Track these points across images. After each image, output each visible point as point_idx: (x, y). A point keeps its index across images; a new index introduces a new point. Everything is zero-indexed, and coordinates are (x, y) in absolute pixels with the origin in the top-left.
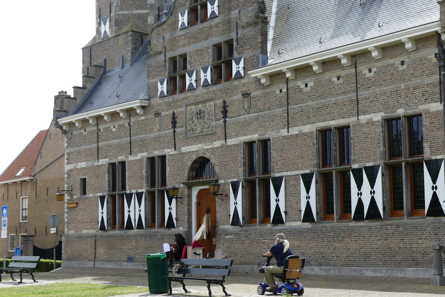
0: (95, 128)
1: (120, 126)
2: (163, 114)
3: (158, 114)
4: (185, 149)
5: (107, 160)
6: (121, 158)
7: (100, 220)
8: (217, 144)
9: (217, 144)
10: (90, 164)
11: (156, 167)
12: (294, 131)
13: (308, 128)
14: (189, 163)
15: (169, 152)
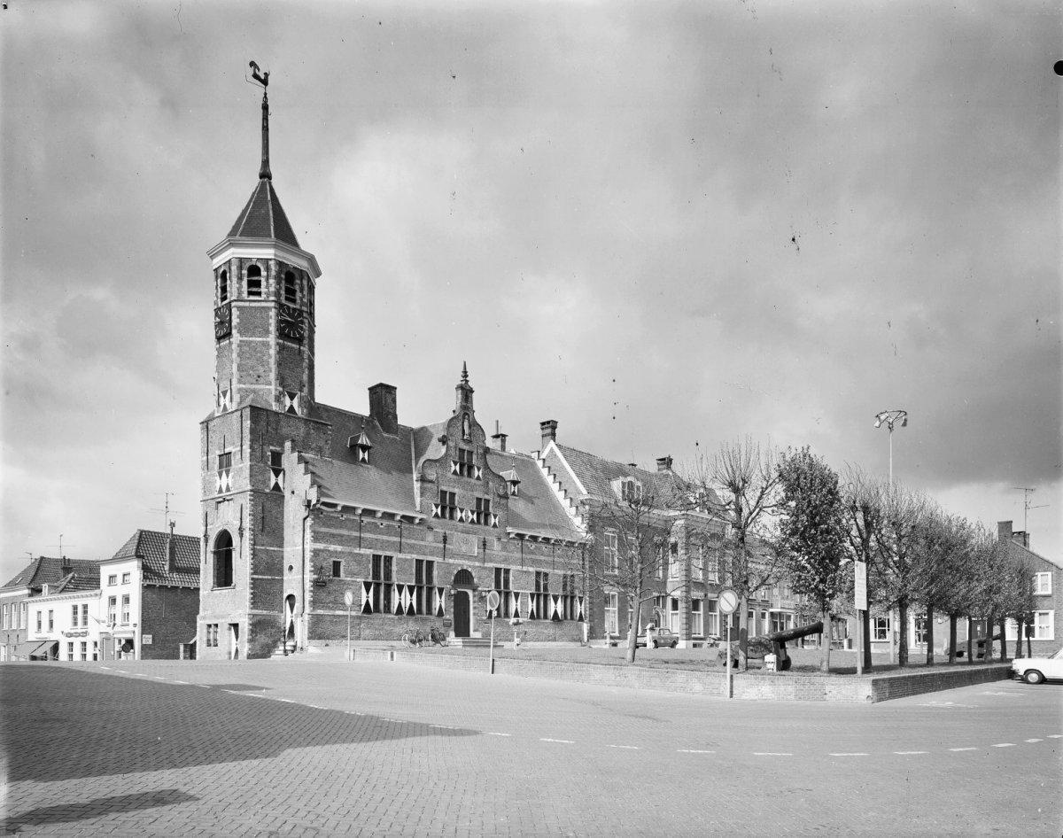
0: (358, 518)
1: (388, 526)
2: (435, 530)
3: (430, 528)
4: (451, 561)
5: (372, 551)
6: (388, 553)
7: (364, 603)
8: (477, 564)
9: (477, 564)
10: (347, 549)
11: (424, 569)
12: (525, 569)
13: (531, 569)
14: (455, 572)
15: (437, 559)
